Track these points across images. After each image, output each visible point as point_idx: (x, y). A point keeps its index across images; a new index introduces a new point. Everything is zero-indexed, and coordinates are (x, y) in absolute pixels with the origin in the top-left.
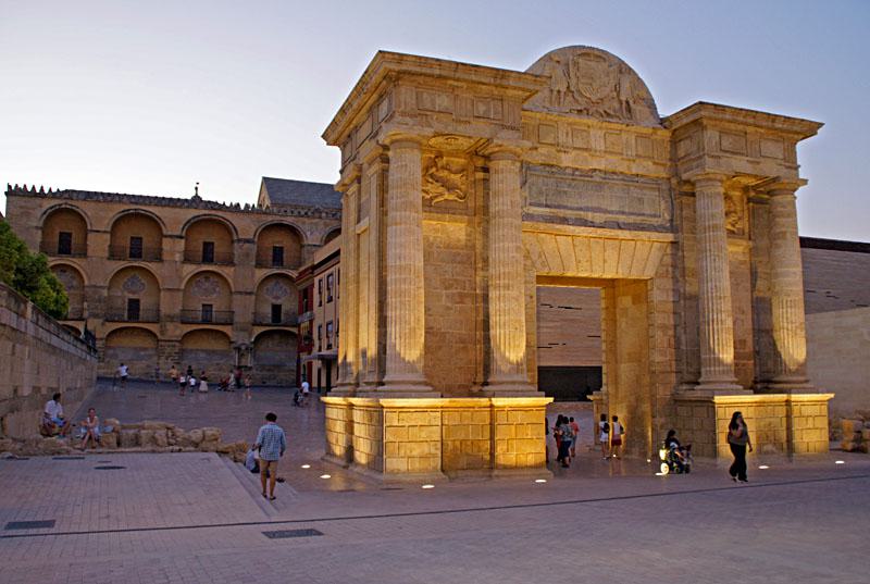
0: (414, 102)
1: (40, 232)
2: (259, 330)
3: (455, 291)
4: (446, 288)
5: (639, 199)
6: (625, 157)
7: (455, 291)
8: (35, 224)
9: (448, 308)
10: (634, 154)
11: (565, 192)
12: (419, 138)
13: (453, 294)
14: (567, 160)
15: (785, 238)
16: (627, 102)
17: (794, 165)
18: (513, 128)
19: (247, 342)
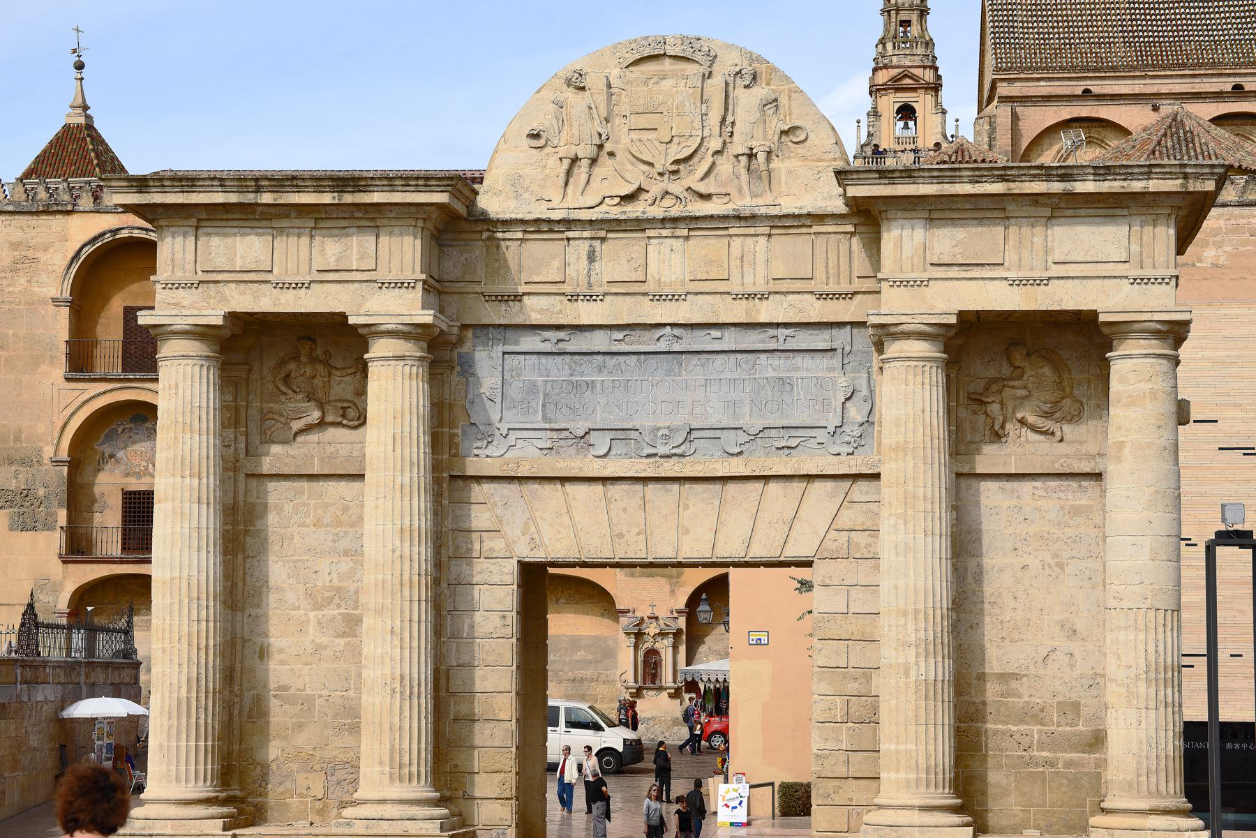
0: (190, 257)
1: (65, 312)
3: (336, 612)
4: (317, 607)
5: (782, 381)
6: (738, 289)
7: (336, 612)
8: (53, 292)
9: (319, 648)
11: (591, 385)
12: (199, 329)
13: (333, 619)
14: (587, 313)
15: (1119, 459)
18: (399, 285)
19: (662, 613)
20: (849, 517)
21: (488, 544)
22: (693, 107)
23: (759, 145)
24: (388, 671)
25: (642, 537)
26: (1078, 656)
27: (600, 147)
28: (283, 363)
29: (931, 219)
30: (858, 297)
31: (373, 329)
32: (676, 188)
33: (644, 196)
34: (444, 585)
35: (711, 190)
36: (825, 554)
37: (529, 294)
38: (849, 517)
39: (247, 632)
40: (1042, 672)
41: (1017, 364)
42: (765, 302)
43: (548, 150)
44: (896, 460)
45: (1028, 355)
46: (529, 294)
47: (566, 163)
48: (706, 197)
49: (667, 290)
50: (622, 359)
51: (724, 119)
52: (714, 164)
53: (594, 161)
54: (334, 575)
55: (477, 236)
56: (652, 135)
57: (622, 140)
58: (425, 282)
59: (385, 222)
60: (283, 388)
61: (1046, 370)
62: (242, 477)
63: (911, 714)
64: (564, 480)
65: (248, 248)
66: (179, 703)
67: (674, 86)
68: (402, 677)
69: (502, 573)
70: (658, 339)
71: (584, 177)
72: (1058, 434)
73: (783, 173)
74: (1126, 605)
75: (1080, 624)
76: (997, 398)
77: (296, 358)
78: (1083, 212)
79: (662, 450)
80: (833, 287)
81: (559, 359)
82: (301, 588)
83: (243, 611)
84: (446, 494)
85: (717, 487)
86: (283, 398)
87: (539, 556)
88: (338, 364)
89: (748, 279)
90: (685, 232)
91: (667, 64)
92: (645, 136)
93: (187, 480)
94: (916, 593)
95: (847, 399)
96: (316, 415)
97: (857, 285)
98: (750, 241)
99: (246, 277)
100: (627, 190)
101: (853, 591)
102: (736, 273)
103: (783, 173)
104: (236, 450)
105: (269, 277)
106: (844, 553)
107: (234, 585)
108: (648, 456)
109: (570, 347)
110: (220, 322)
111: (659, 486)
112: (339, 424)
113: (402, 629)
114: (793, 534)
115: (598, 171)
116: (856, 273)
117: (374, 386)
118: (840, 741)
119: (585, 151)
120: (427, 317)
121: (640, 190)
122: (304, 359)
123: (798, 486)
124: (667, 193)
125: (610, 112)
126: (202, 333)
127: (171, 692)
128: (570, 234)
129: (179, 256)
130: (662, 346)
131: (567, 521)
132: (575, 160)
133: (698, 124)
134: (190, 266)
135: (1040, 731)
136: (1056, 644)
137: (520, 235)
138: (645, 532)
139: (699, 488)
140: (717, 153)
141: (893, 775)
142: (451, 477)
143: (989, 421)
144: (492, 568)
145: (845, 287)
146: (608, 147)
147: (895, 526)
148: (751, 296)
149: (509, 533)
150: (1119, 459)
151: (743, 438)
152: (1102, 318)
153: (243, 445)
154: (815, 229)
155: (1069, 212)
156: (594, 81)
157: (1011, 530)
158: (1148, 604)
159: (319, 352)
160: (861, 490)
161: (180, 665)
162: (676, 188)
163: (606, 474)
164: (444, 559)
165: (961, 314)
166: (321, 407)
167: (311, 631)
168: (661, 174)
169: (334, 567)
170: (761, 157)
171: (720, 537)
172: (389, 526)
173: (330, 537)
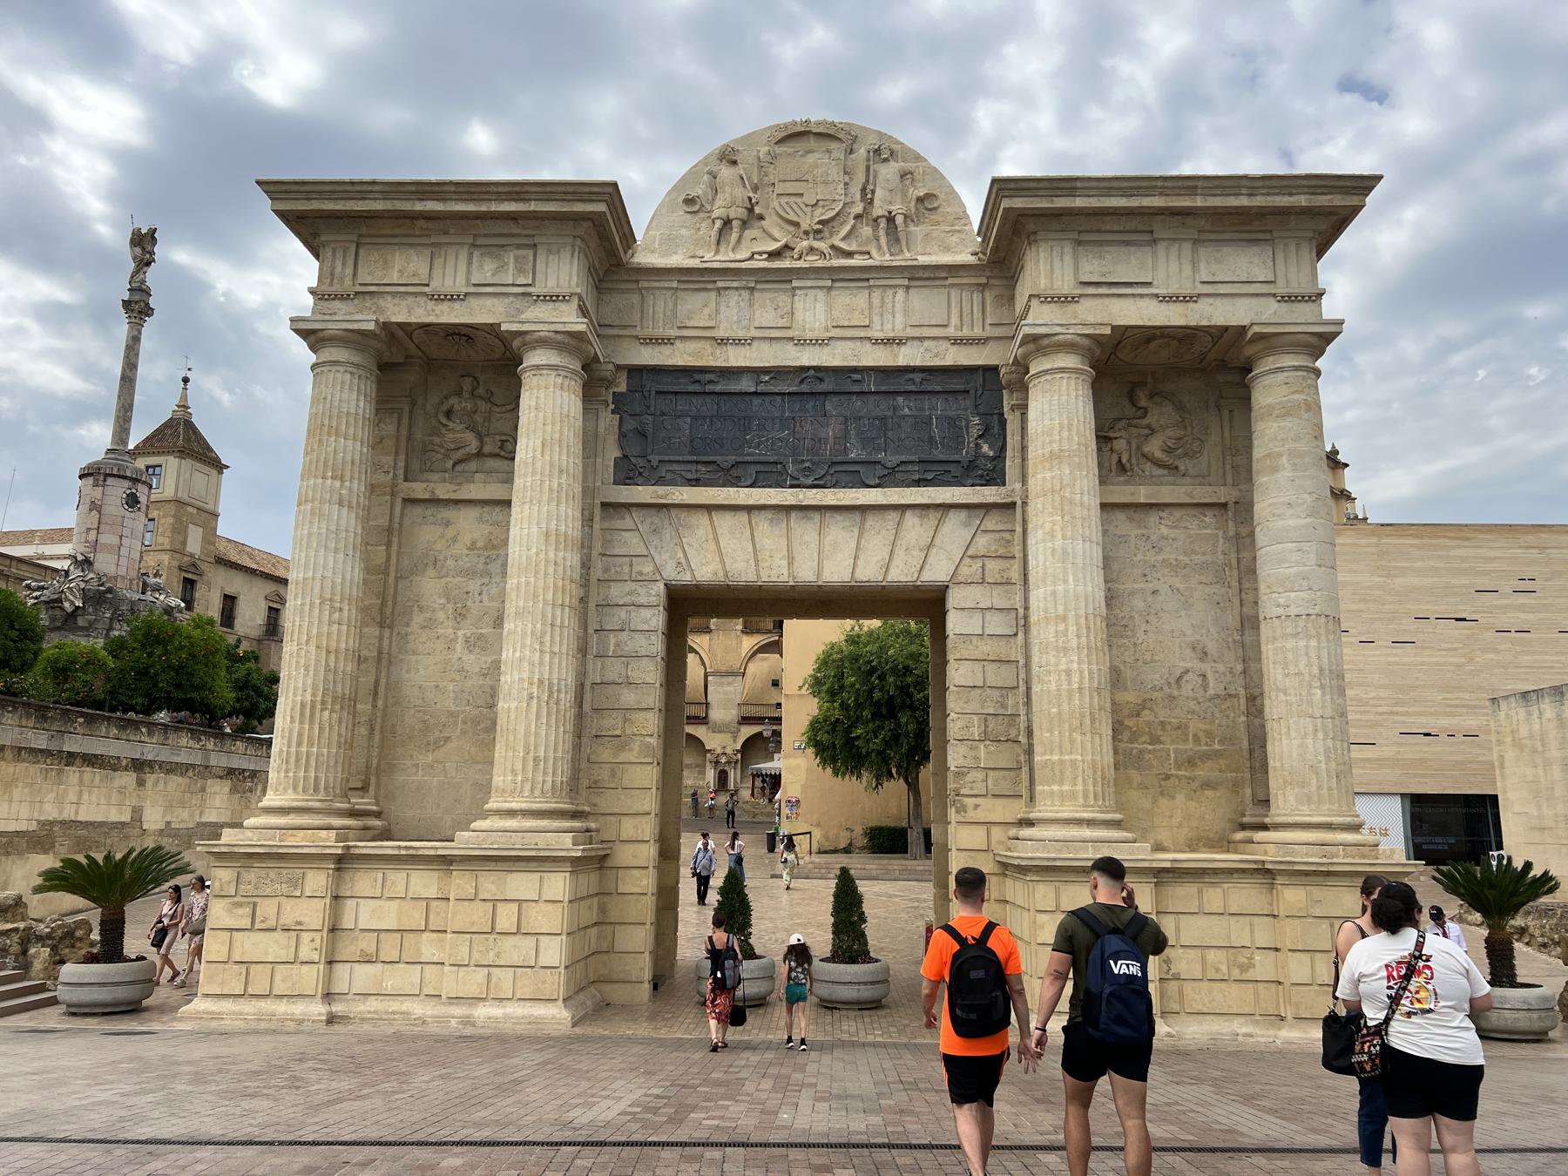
0: (349, 271)
2: (748, 731)
10: (899, 326)
16: (891, 219)
17: (1307, 289)
18: (553, 298)
19: (729, 751)
20: (982, 543)
21: (636, 569)
22: (835, 173)
23: (897, 208)
24: (525, 676)
25: (785, 563)
26: (1210, 676)
27: (751, 210)
28: (446, 398)
29: (1080, 243)
30: (991, 344)
31: (528, 338)
32: (822, 245)
33: (788, 254)
34: (592, 605)
35: (853, 248)
36: (961, 579)
37: (683, 338)
38: (982, 543)
39: (394, 650)
40: (1176, 693)
41: (1143, 403)
42: (903, 348)
43: (702, 215)
44: (1051, 469)
45: (1151, 397)
46: (683, 338)
47: (718, 224)
48: (850, 254)
49: (809, 335)
50: (767, 399)
51: (864, 190)
52: (853, 227)
53: (745, 224)
54: (485, 596)
55: (633, 286)
56: (798, 200)
57: (771, 205)
58: (580, 298)
59: (543, 240)
60: (444, 421)
61: (1169, 409)
62: (399, 502)
63: (1076, 723)
64: (709, 508)
65: (405, 265)
66: (303, 705)
67: (821, 161)
68: (541, 682)
69: (649, 595)
70: (802, 382)
71: (735, 236)
72: (1182, 468)
73: (919, 237)
74: (1293, 611)
75: (1212, 647)
76: (1123, 433)
77: (459, 394)
78: (1228, 236)
79: (803, 480)
80: (966, 332)
81: (708, 399)
82: (450, 606)
83: (391, 627)
84: (597, 518)
85: (857, 516)
86: (443, 430)
87: (686, 578)
88: (498, 402)
89: (888, 326)
90: (829, 283)
91: (812, 143)
92: (792, 200)
93: (329, 482)
94: (1077, 598)
95: (980, 437)
96: (474, 445)
97: (989, 332)
98: (890, 292)
99: (402, 289)
100: (774, 246)
101: (988, 615)
102: (876, 319)
103: (919, 237)
104: (395, 476)
106: (978, 578)
107: (384, 604)
108: (792, 486)
109: (718, 388)
110: (371, 326)
111: (801, 514)
112: (497, 455)
113: (544, 633)
114: (930, 560)
115: (749, 233)
116: (989, 321)
117: (527, 400)
118: (977, 758)
119: (738, 212)
120: (580, 325)
121: (786, 247)
122: (466, 395)
123: (933, 516)
124: (812, 250)
125: (761, 180)
126: (354, 339)
127: (295, 694)
128: (720, 284)
129: (339, 269)
130: (805, 388)
131: (713, 547)
132: (727, 222)
133: (840, 189)
134: (348, 281)
135: (1176, 751)
136: (1189, 665)
137: (675, 284)
138: (791, 561)
139: (839, 517)
140: (857, 217)
141: (1055, 788)
142: (603, 504)
143: (1115, 457)
144: (640, 590)
145: (977, 332)
146: (757, 210)
147: (1052, 534)
148: (889, 342)
149: (657, 558)
150: (1275, 469)
151: (880, 471)
152: (1257, 329)
153: (401, 472)
154: (950, 281)
155: (1213, 236)
156: (746, 157)
157: (1140, 557)
158: (1317, 610)
159: (481, 390)
160: (992, 522)
161: (307, 668)
162: (822, 245)
163: (751, 502)
164: (593, 579)
165: (1114, 328)
166: (480, 437)
167: (459, 648)
168: (806, 233)
169: (485, 589)
170: (899, 220)
171: (860, 562)
172: (535, 529)
173: (482, 560)
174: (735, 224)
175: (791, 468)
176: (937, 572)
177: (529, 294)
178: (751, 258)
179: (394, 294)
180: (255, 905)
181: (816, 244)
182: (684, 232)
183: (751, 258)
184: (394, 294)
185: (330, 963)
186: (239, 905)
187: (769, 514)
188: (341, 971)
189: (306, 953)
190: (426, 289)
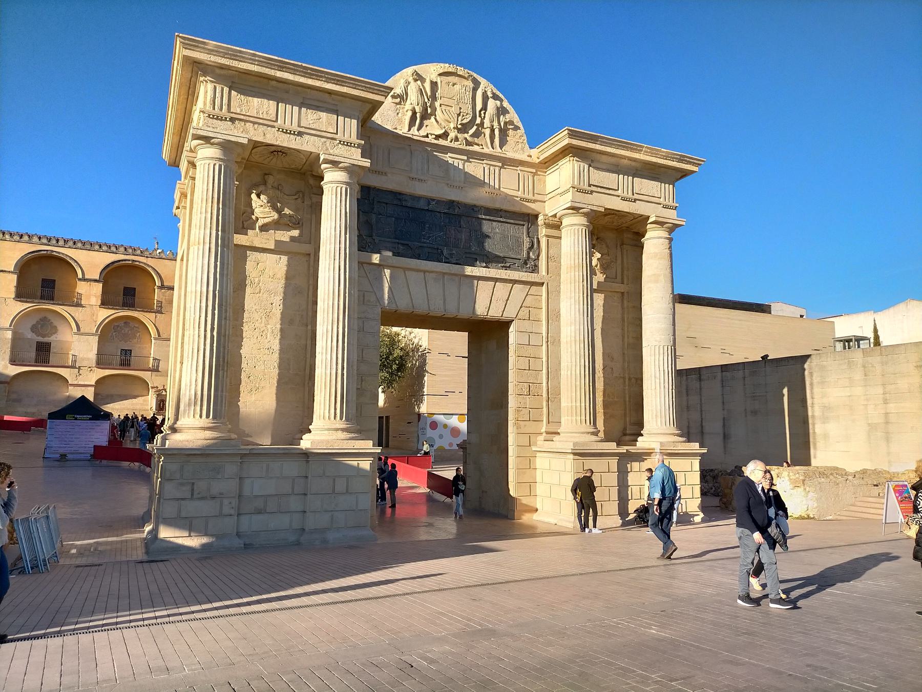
18: (349, 144)
100: (441, 132)
105: (275, 124)
110: (245, 141)
115: (426, 122)
165: (606, 209)
174: (418, 115)
175: (445, 252)
176: (509, 314)
177: (335, 139)
178: (427, 136)
179: (254, 123)
180: (193, 484)
181: (459, 136)
182: (390, 112)
183: (427, 136)
184: (254, 123)
185: (239, 515)
186: (182, 484)
187: (434, 275)
188: (244, 519)
189: (226, 510)
190: (275, 124)
